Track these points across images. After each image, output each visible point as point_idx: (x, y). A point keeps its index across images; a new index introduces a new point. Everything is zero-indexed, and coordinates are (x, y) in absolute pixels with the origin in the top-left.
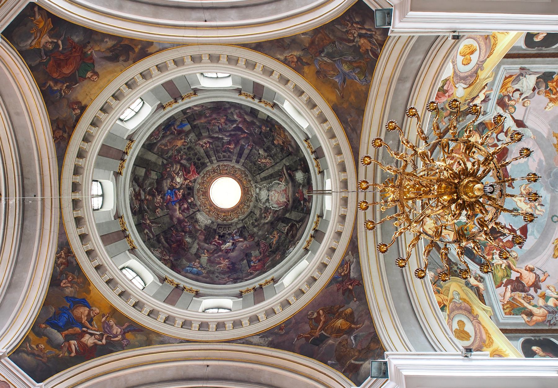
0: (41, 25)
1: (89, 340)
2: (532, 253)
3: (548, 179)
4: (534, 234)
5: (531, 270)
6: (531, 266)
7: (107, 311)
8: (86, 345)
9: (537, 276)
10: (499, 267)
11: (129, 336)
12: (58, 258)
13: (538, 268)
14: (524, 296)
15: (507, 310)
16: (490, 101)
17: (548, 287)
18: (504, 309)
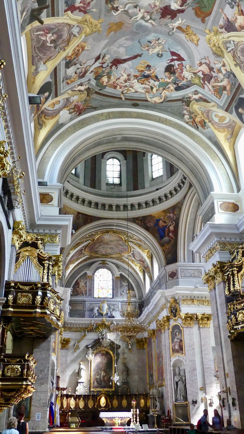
2: (191, 57)
3: (140, 34)
4: (178, 50)
5: (201, 64)
6: (198, 62)
7: (163, 214)
8: (173, 230)
9: (206, 63)
10: (193, 79)
11: (175, 213)
12: (138, 224)
13: (202, 59)
14: (214, 80)
15: (218, 96)
16: (82, 82)
17: (215, 64)
18: (217, 97)
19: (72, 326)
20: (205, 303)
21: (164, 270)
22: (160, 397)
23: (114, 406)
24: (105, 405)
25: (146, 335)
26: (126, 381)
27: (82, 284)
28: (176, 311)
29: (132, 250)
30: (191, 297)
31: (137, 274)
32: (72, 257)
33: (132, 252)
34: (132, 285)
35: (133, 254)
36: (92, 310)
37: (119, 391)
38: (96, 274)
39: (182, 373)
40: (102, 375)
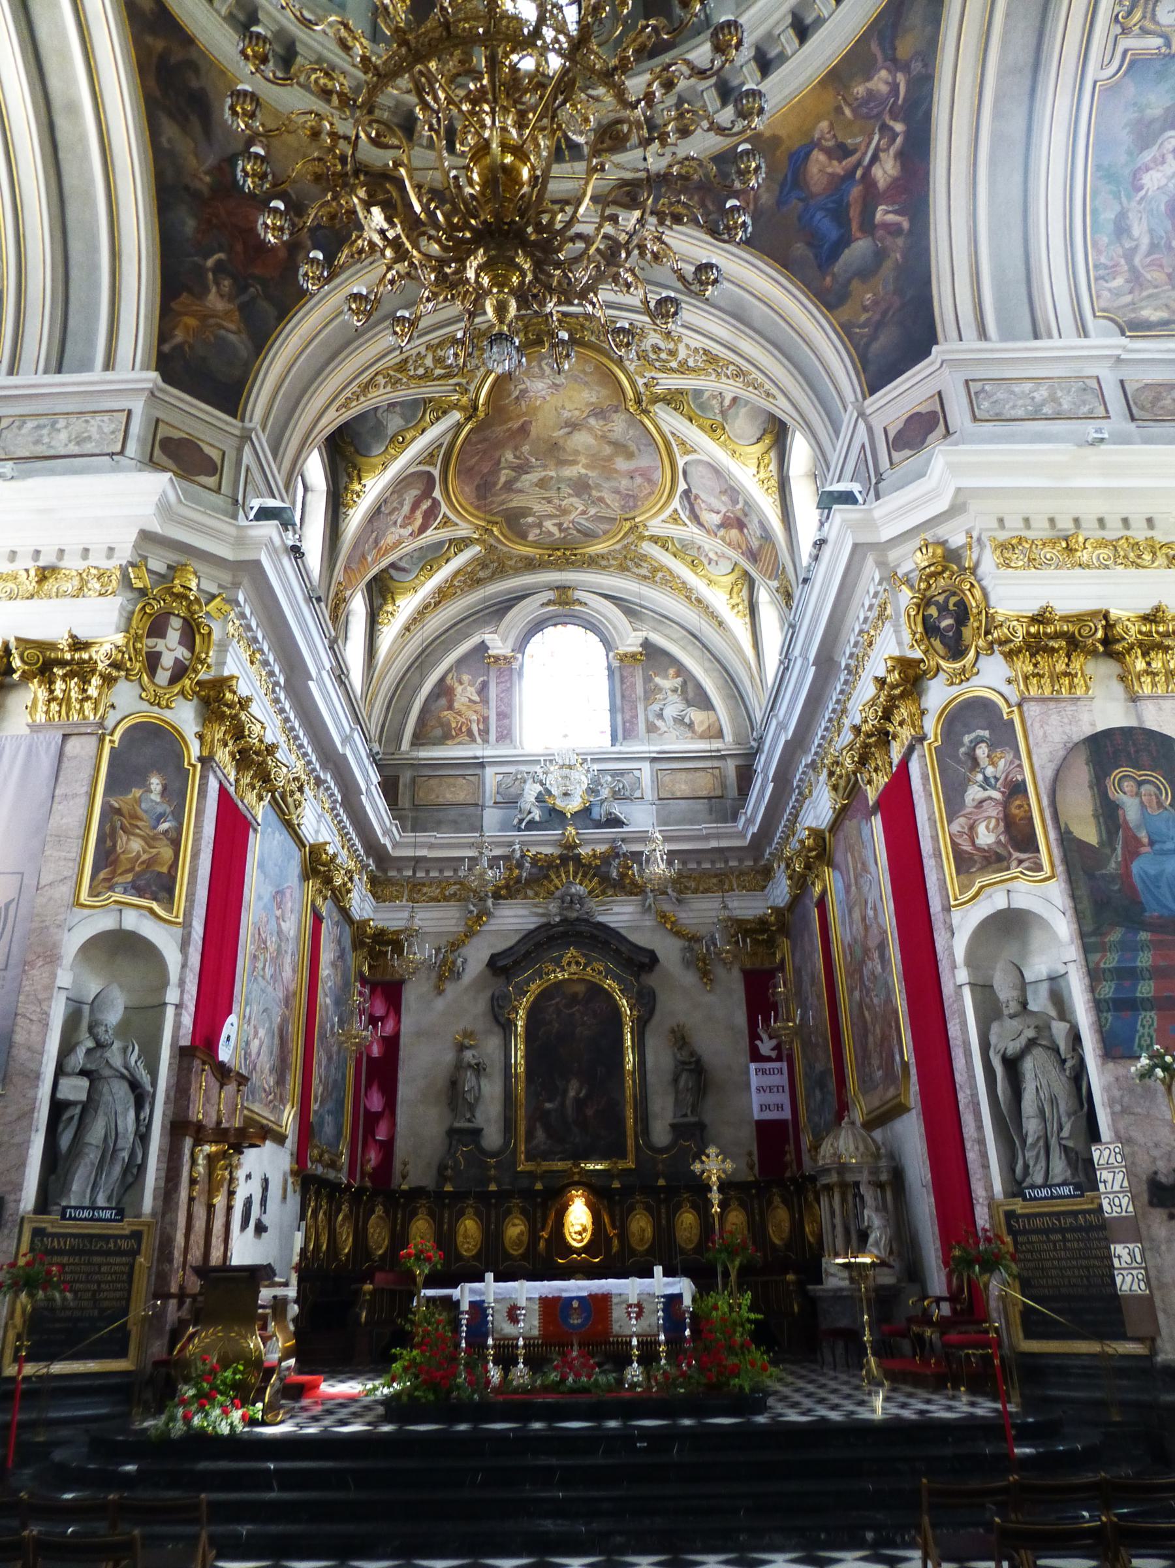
0: (192, 322)
1: (886, 171)
8: (896, 180)
19: (420, 874)
20: (1147, 557)
21: (862, 425)
22: (884, 1177)
23: (634, 1242)
24: (591, 1242)
25: (781, 891)
26: (692, 1119)
27: (465, 693)
28: (962, 614)
29: (681, 463)
30: (1052, 521)
31: (720, 624)
32: (376, 513)
33: (682, 486)
34: (699, 687)
35: (687, 493)
36: (510, 801)
37: (660, 1166)
38: (531, 648)
39: (1039, 1002)
40: (572, 1093)
